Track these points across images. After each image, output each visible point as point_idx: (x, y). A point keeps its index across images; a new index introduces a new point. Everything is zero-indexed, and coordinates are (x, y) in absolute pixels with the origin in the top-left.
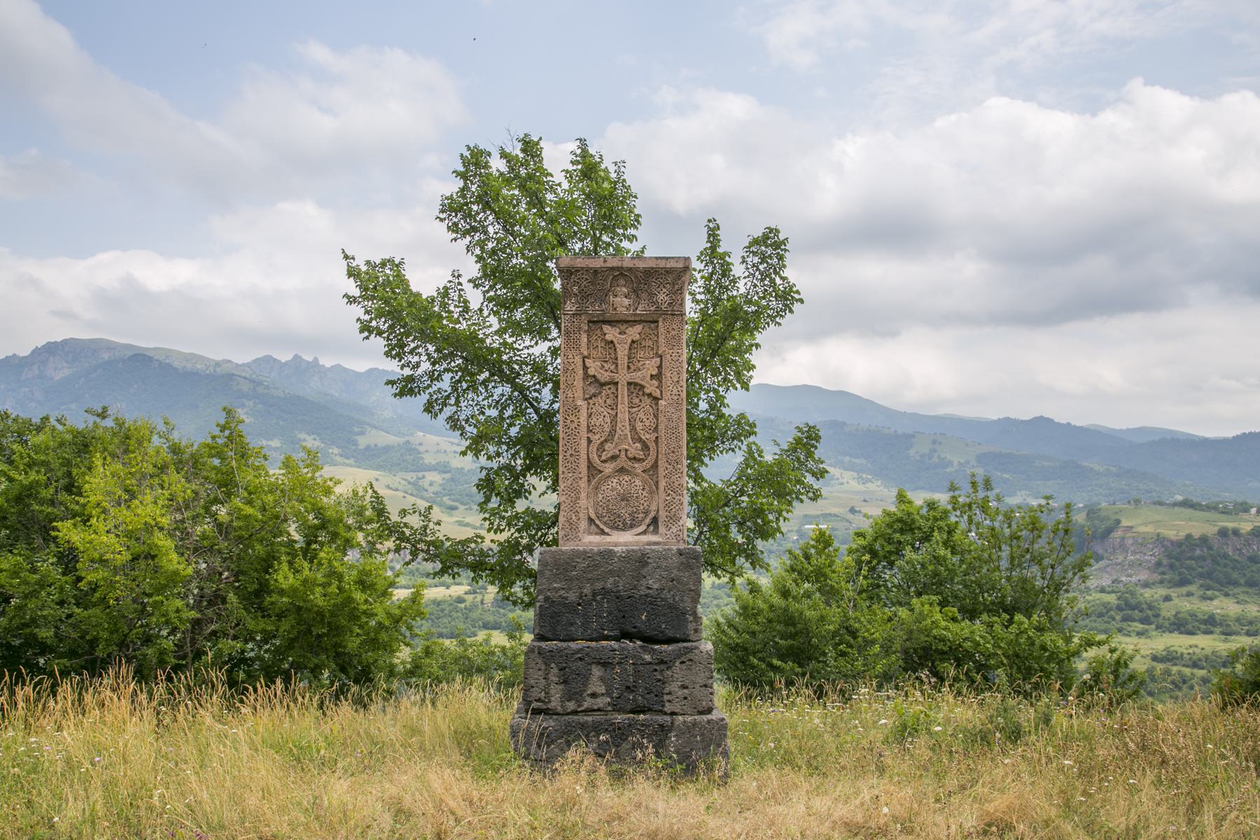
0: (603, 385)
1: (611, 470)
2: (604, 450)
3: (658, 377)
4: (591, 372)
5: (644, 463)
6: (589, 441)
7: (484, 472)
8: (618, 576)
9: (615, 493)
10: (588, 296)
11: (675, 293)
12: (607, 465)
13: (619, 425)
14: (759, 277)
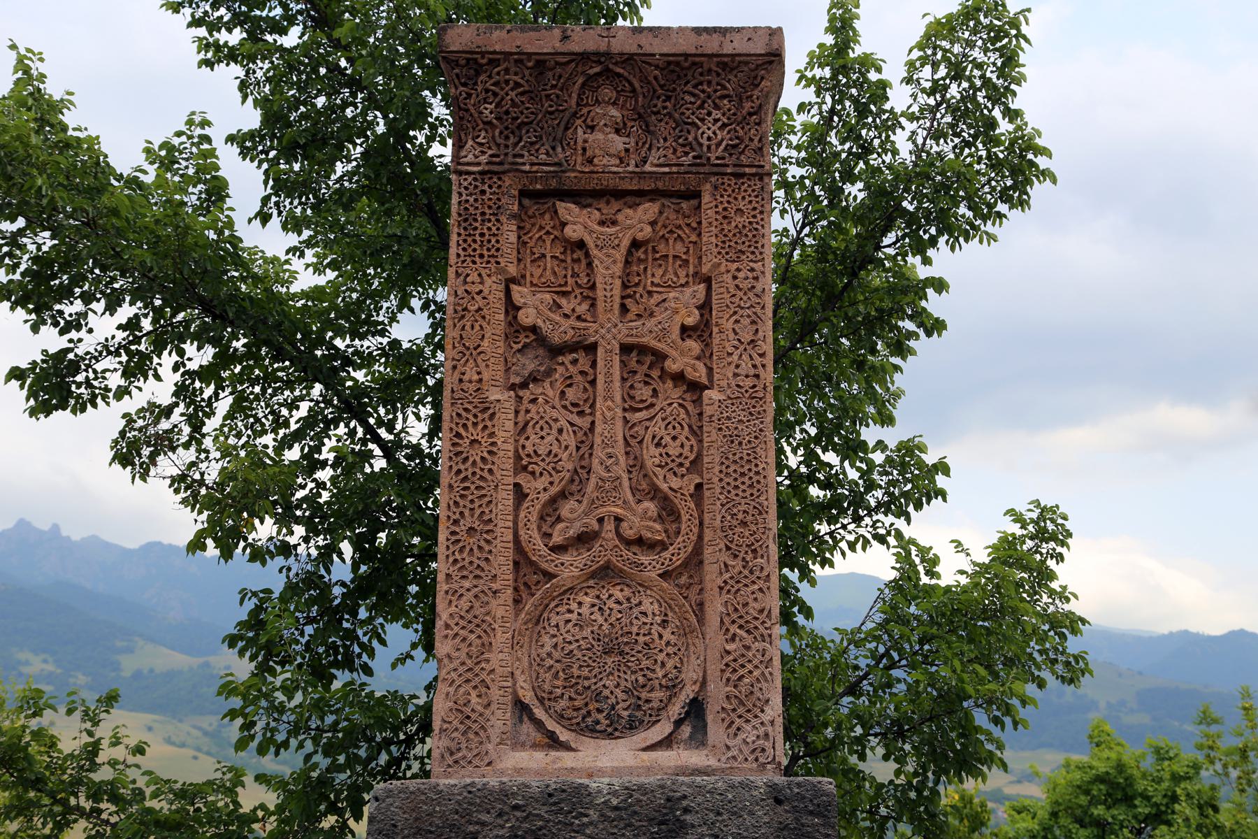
0: (556, 351)
1: (576, 572)
2: (559, 520)
3: (699, 331)
4: (527, 317)
5: (666, 554)
6: (520, 495)
7: (250, 604)
9: (587, 632)
10: (519, 127)
11: (743, 122)
12: (566, 558)
13: (599, 453)
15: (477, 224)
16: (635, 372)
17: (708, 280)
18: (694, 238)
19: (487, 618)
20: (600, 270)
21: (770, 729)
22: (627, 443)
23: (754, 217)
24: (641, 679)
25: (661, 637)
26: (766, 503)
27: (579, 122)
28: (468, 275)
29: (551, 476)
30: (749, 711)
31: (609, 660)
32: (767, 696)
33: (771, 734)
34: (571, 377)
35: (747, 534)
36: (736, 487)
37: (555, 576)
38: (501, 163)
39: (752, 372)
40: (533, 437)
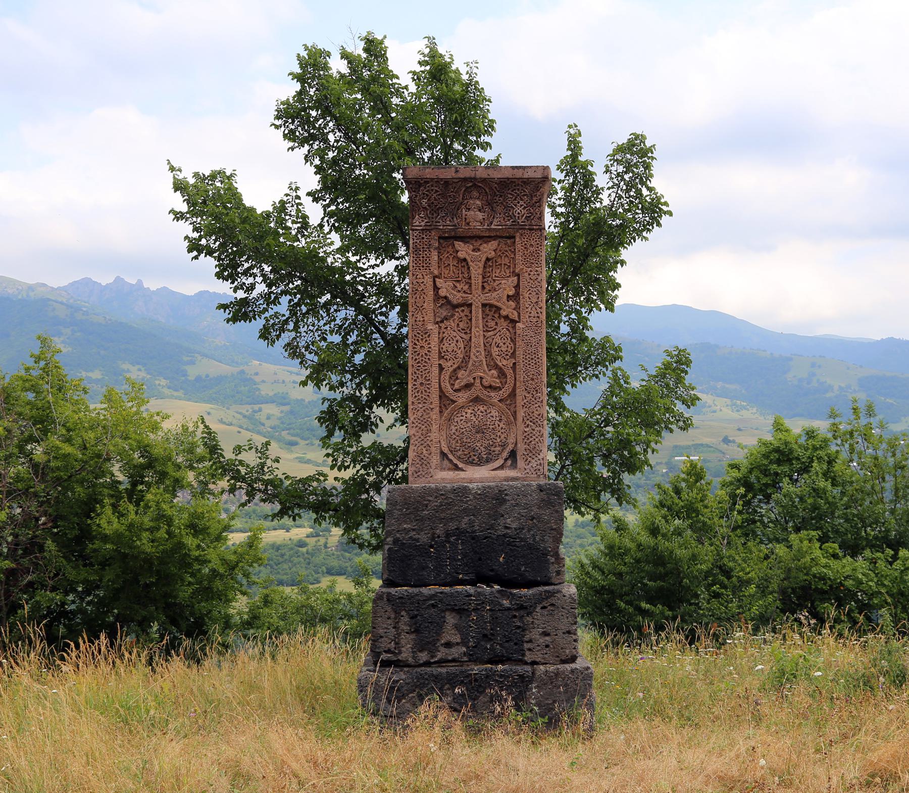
0: (455, 307)
1: (464, 400)
2: (457, 378)
3: (515, 297)
4: (443, 293)
5: (501, 392)
6: (441, 368)
8: (473, 515)
9: (469, 424)
10: (438, 209)
12: (460, 394)
13: (473, 350)
14: (625, 188)
17: (518, 275)
18: (512, 256)
20: (473, 271)
21: (542, 462)
22: (485, 346)
24: (491, 443)
27: (463, 206)
31: (478, 435)
36: (529, 364)
39: (536, 315)
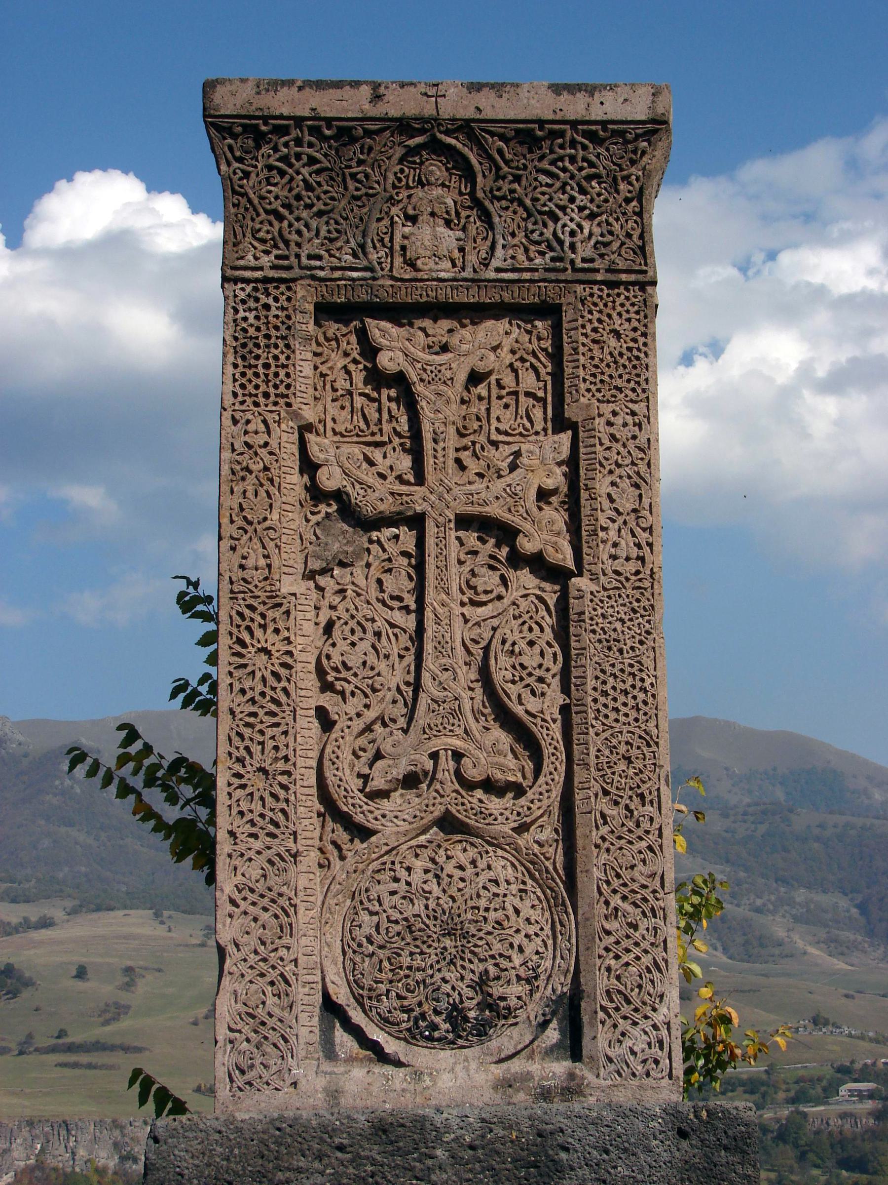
4: (330, 480)
9: (419, 907)
15: (260, 352)
16: (475, 553)
19: (284, 889)
23: (635, 340)
24: (493, 971)
25: (517, 912)
26: (654, 732)
28: (248, 422)
29: (366, 696)
30: (636, 1010)
32: (660, 989)
33: (666, 1040)
34: (390, 560)
35: (631, 772)
37: (372, 833)
38: (289, 268)
40: (340, 643)
